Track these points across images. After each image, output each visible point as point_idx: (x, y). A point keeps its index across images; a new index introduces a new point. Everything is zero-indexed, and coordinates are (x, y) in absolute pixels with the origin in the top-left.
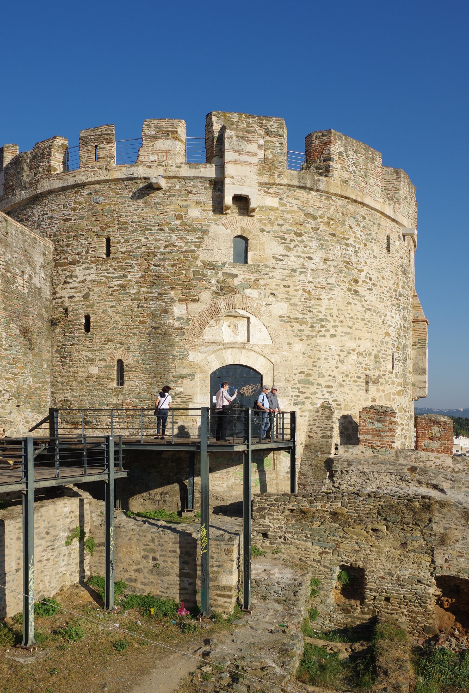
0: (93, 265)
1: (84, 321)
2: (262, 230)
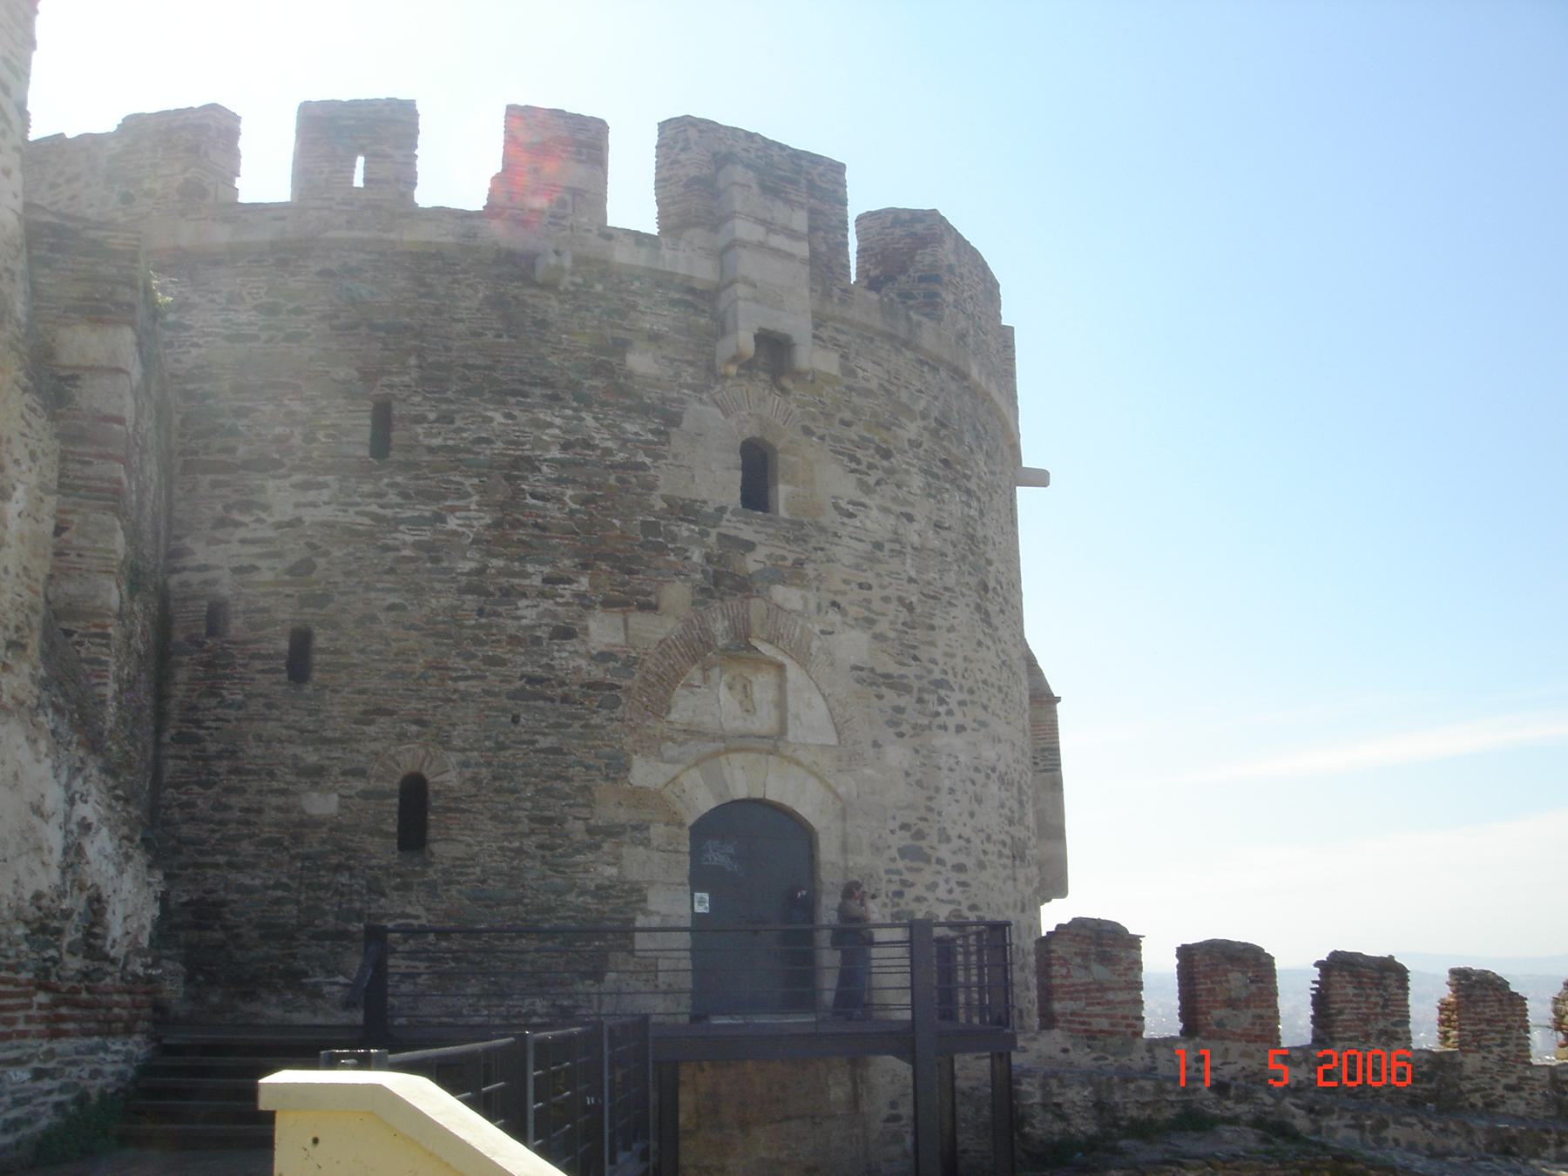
0: (329, 478)
2: (807, 431)
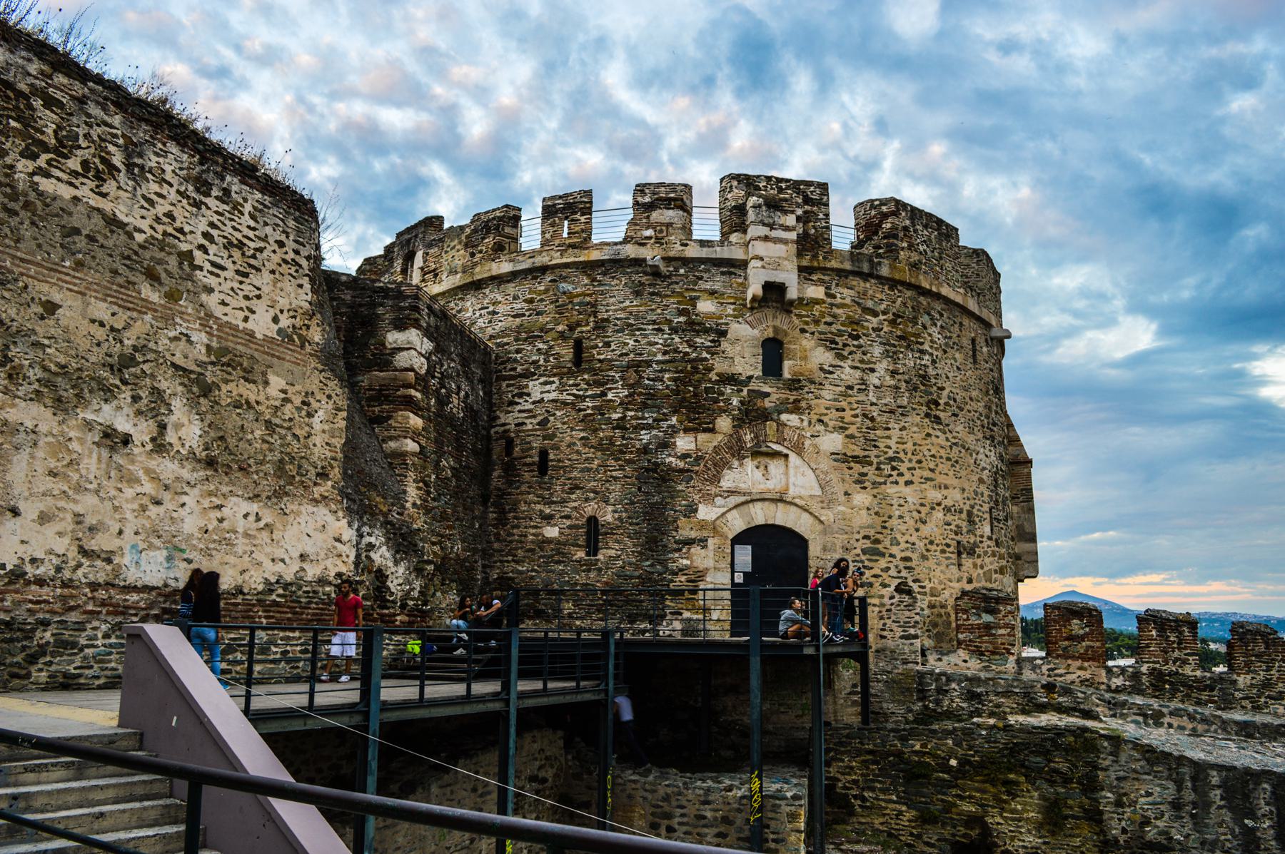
0: (555, 379)
1: (536, 459)
